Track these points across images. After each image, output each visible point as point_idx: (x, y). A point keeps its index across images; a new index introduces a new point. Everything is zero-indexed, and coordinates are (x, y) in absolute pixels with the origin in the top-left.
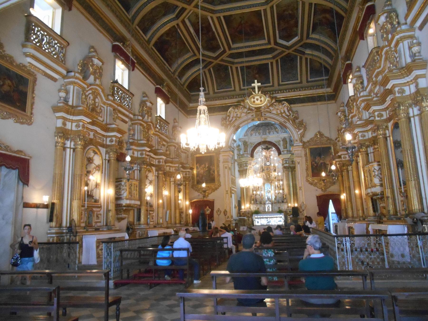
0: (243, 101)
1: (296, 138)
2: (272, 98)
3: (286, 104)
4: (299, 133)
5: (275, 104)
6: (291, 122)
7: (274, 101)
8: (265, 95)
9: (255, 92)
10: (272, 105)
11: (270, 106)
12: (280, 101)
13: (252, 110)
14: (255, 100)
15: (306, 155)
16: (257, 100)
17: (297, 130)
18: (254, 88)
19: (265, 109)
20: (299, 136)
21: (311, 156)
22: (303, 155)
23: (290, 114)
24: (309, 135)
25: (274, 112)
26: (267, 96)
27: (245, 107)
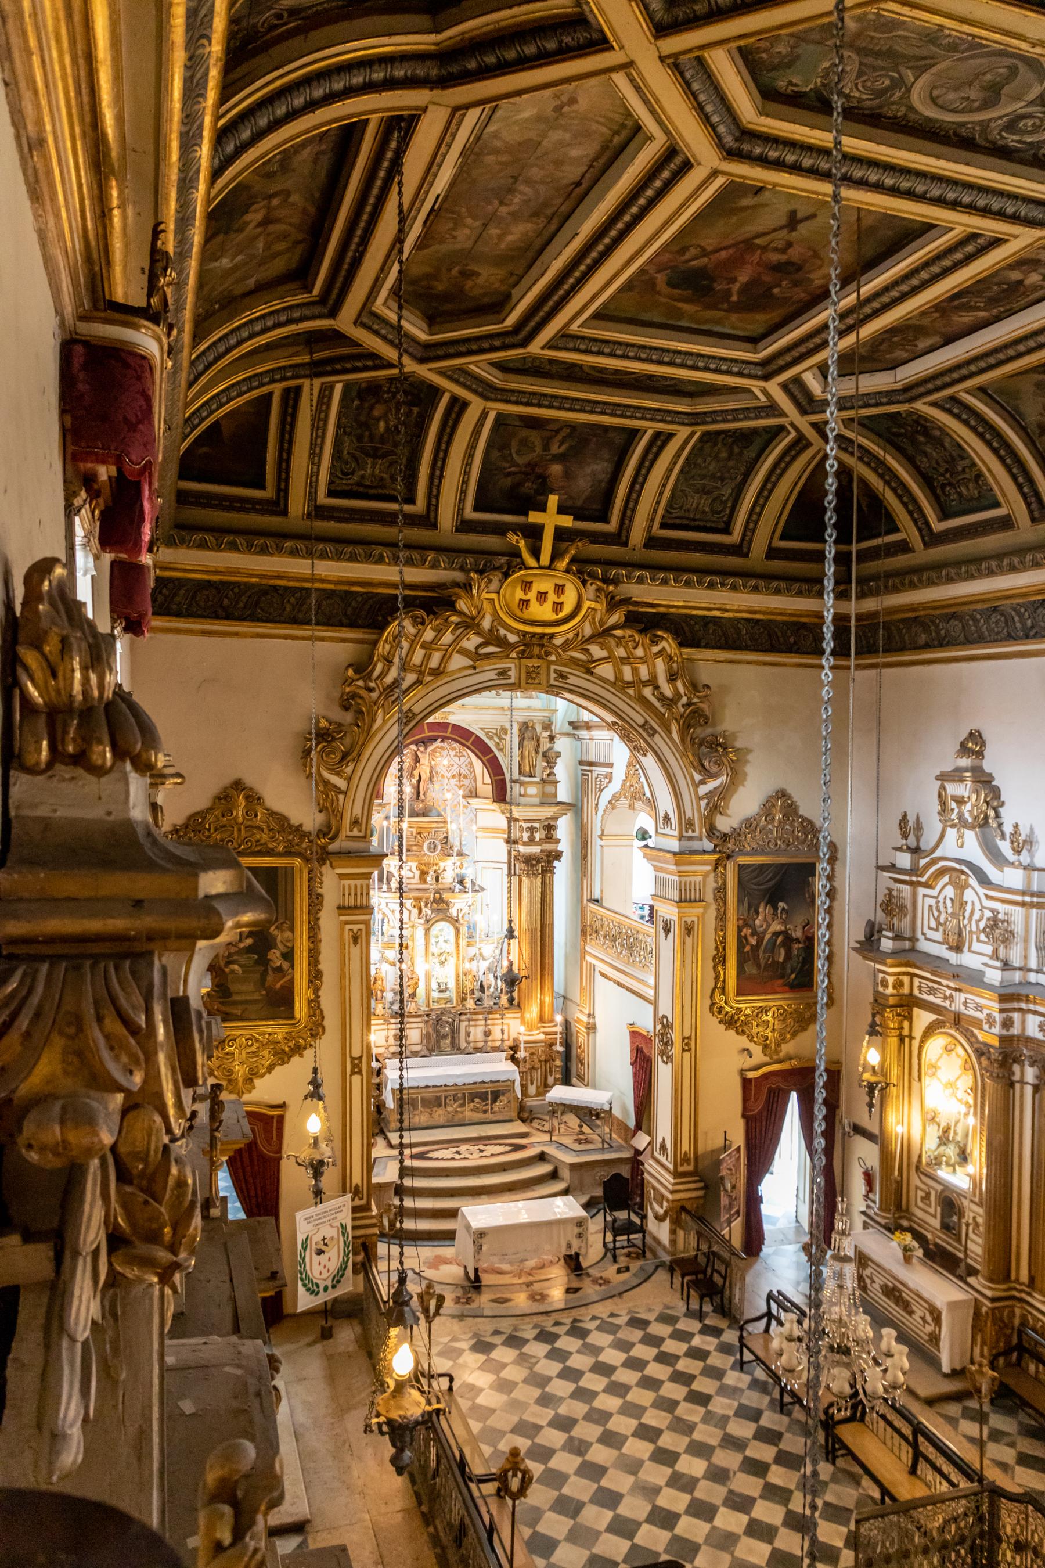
0: (467, 587)
1: (689, 814)
2: (613, 604)
3: (668, 644)
4: (703, 790)
5: (618, 633)
6: (675, 735)
7: (616, 617)
8: (584, 582)
9: (536, 553)
10: (603, 634)
11: (591, 639)
12: (647, 622)
13: (502, 642)
14: (532, 596)
15: (720, 891)
16: (542, 596)
17: (697, 777)
18: (534, 533)
19: (566, 645)
20: (703, 803)
21: (740, 901)
22: (709, 897)
23: (678, 695)
24: (745, 804)
27: (470, 624)
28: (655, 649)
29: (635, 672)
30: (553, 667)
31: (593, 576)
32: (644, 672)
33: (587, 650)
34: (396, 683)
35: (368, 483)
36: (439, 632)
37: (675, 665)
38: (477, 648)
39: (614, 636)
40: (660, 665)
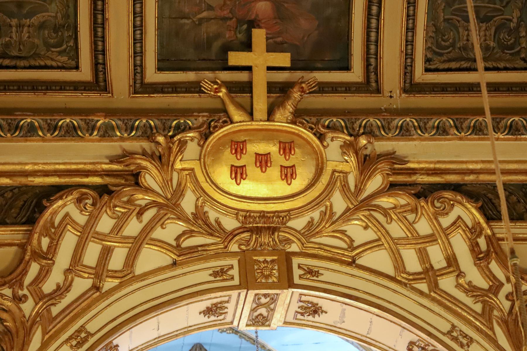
8: (321, 137)
11: (348, 215)
13: (212, 229)
25: (380, 260)
26: (334, 145)
28: (446, 221)
29: (423, 256)
30: (296, 261)
31: (331, 128)
32: (437, 256)
33: (343, 232)
34: (61, 291)
35: (15, 53)
36: (121, 221)
37: (482, 242)
38: (178, 239)
39: (378, 208)
40: (460, 245)
